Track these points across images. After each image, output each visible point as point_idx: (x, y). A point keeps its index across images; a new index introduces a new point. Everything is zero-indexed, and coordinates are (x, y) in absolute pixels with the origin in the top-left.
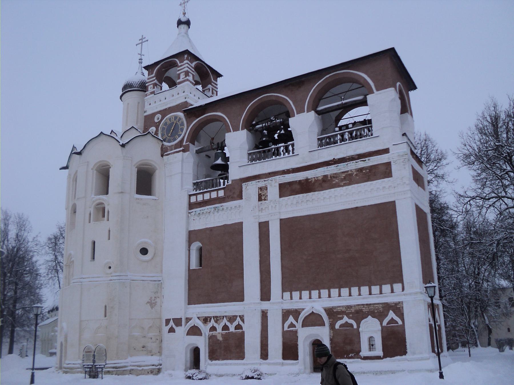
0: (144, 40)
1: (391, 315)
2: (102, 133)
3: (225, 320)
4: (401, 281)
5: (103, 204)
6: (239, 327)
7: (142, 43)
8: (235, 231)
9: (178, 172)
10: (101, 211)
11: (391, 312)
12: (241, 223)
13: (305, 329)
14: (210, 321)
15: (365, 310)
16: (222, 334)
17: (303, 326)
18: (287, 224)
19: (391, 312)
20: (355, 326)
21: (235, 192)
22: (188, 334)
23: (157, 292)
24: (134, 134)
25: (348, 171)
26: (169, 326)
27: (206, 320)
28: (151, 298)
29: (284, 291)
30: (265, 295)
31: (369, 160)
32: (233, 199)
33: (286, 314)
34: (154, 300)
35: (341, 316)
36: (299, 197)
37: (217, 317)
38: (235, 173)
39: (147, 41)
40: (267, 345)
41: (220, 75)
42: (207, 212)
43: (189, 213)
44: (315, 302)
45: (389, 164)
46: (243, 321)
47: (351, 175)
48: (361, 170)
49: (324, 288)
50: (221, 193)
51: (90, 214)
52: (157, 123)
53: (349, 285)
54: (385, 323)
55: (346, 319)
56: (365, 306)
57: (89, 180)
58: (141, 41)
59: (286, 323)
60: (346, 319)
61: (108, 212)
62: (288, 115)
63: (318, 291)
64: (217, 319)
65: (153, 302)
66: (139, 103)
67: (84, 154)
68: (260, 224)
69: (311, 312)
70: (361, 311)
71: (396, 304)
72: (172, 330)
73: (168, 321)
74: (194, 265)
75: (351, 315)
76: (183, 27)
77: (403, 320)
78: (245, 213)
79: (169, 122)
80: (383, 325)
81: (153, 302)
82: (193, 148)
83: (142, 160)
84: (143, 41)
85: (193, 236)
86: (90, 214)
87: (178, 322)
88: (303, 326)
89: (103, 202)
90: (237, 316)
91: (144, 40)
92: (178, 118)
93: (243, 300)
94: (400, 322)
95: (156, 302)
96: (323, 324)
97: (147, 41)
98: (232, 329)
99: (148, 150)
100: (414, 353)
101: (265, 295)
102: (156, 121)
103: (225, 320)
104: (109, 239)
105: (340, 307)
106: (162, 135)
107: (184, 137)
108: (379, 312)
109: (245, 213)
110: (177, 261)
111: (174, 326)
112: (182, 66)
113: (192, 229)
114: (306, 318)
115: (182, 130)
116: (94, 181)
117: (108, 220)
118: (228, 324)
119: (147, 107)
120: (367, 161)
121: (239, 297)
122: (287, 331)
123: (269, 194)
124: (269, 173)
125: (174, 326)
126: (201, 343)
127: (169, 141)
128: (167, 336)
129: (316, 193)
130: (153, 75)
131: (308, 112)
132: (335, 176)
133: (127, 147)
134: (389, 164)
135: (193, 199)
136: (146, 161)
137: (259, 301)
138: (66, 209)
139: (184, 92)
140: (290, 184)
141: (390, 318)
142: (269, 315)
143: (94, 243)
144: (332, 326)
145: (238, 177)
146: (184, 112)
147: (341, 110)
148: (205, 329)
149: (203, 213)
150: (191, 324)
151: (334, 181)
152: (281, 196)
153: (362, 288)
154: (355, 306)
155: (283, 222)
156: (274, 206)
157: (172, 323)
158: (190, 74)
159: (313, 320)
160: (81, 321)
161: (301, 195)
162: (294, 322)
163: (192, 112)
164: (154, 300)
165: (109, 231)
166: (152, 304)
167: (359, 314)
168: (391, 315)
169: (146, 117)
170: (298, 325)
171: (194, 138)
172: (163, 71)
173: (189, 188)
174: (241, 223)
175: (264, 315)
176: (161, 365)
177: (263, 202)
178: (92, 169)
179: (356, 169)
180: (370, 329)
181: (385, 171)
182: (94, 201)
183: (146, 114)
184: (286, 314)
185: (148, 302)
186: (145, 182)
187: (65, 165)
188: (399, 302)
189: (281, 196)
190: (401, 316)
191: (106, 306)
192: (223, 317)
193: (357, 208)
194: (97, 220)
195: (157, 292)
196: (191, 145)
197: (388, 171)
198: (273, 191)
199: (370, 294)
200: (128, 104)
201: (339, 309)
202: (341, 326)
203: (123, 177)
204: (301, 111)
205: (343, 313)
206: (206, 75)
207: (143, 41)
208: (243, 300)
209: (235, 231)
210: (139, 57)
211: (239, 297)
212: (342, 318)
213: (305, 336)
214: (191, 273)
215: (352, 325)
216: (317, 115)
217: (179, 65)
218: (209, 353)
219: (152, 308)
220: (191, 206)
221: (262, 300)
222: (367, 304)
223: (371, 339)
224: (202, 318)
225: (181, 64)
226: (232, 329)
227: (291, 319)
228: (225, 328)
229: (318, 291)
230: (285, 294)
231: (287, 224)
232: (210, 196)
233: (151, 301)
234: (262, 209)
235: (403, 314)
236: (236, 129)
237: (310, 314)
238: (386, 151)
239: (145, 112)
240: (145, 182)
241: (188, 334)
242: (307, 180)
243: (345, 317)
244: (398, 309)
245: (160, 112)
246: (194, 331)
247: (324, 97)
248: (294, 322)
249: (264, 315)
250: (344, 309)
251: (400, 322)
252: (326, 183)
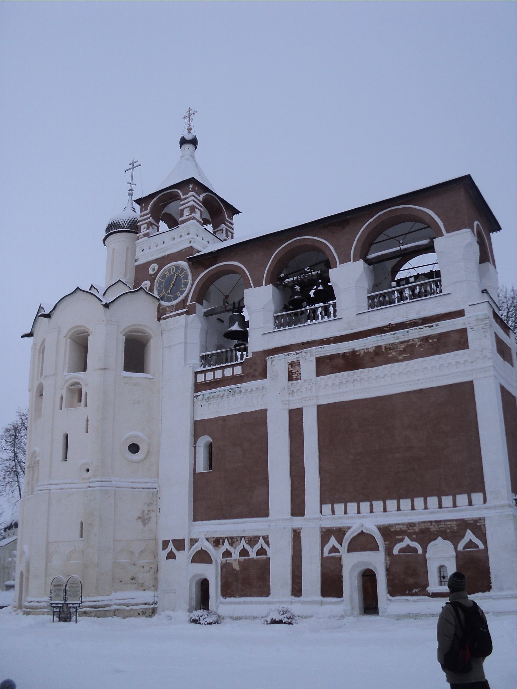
0: (135, 165)
1: (469, 536)
2: (78, 288)
3: (243, 543)
5: (79, 384)
6: (262, 552)
7: (132, 168)
8: (257, 421)
9: (180, 342)
10: (77, 394)
11: (469, 532)
12: (266, 410)
13: (352, 554)
14: (223, 544)
15: (433, 528)
16: (239, 562)
17: (349, 551)
18: (325, 412)
19: (469, 532)
20: (420, 551)
21: (256, 369)
22: (193, 561)
23: (151, 504)
24: (122, 289)
25: (408, 341)
26: (168, 550)
27: (217, 542)
28: (143, 511)
29: (323, 502)
30: (298, 508)
31: (437, 325)
32: (254, 378)
33: (326, 534)
34: (148, 514)
35: (401, 537)
36: (343, 375)
37: (232, 538)
38: (256, 343)
39: (140, 165)
40: (300, 577)
41: (238, 212)
42: (218, 396)
43: (195, 397)
44: (366, 518)
45: (464, 331)
46: (268, 543)
48: (426, 339)
49: (377, 499)
50: (238, 370)
51: (62, 398)
52: (152, 275)
53: (411, 495)
54: (460, 547)
55: (407, 541)
56: (433, 524)
57: (62, 352)
58: (131, 166)
59: (327, 546)
60: (407, 541)
61: (86, 395)
62: (328, 264)
63: (368, 503)
64: (232, 541)
65: (146, 517)
66: (128, 248)
67: (54, 317)
68: (291, 412)
69: (359, 531)
70: (428, 529)
71: (476, 521)
72: (171, 556)
73: (166, 544)
74: (201, 468)
75: (414, 536)
76: (188, 147)
77: (485, 543)
78: (271, 397)
79: (168, 274)
80: (458, 550)
81: (146, 517)
82: (201, 309)
83: (133, 325)
84: (134, 165)
85: (199, 428)
86: (62, 398)
87: (179, 544)
88: (349, 551)
89: (78, 381)
90: (259, 537)
91: (135, 165)
92: (180, 269)
93: (267, 515)
94: (481, 546)
95: (150, 518)
96: (377, 549)
97: (140, 165)
98: (253, 554)
99: (140, 312)
100: (501, 589)
101: (298, 508)
102: (151, 272)
103: (243, 543)
104: (87, 432)
105: (399, 524)
106: (159, 292)
108: (452, 532)
109: (271, 397)
110: (178, 462)
111: (174, 550)
112: (186, 199)
113: (198, 418)
114: (354, 539)
115: (186, 285)
116: (68, 355)
117: (86, 406)
118: (248, 547)
119: (139, 254)
120: (435, 327)
121: (262, 510)
122: (327, 558)
123: (302, 372)
124: (303, 344)
125: (174, 550)
126: (211, 573)
127: (168, 300)
128: (164, 564)
129: (366, 370)
130: (148, 211)
131: (354, 261)
132: (390, 347)
133: (112, 307)
134: (464, 331)
135: (200, 378)
136: (138, 327)
137: (289, 516)
138: (29, 391)
139: (188, 234)
140: (331, 358)
141: (468, 540)
142: (303, 535)
143: (67, 437)
144: (389, 551)
145: (260, 349)
146: (189, 260)
147: (399, 259)
148: (216, 554)
149: (213, 396)
150: (197, 547)
151: (391, 353)
152: (318, 375)
153: (429, 499)
154: (419, 523)
156: (309, 387)
157: (171, 546)
158: (196, 210)
159: (363, 542)
160: (48, 543)
161: (345, 373)
162: (337, 546)
163: (199, 262)
164: (148, 514)
165: (88, 421)
166: (144, 519)
168: (469, 536)
169: (137, 267)
170: (343, 550)
171: (201, 295)
172: (161, 206)
173: (195, 362)
174: (266, 410)
175: (297, 535)
176: (156, 603)
177: (295, 382)
178: (65, 337)
179: (419, 338)
181: (459, 341)
182: (67, 381)
183: (137, 263)
184: (326, 534)
185: (139, 518)
186: (136, 354)
187: (29, 332)
188: (480, 519)
189: (318, 375)
190: (483, 537)
191: (82, 523)
192: (241, 538)
193: (421, 389)
194: (71, 405)
195: (151, 504)
196: (197, 304)
197: (462, 340)
199: (440, 507)
200: (114, 249)
201: (398, 528)
202: (401, 551)
203: (106, 347)
204: (345, 259)
205: (403, 533)
206: (218, 211)
207: (134, 165)
208: (267, 515)
209: (257, 421)
210: (129, 187)
211: (262, 510)
212: (402, 540)
213: (352, 564)
214: (197, 477)
215: (415, 550)
216: (366, 265)
217: (182, 197)
218: (222, 587)
219: (144, 525)
220: (198, 387)
221: (294, 514)
222: (436, 522)
224: (213, 540)
225: (185, 196)
226: (253, 554)
227: (333, 541)
228: (244, 553)
229: (368, 503)
230: (324, 506)
231: (325, 412)
232: (223, 374)
233: (144, 516)
234: (293, 391)
235: (485, 535)
236: (258, 284)
237: (359, 535)
238: (460, 313)
239: (136, 260)
240: (136, 354)
241: (193, 561)
242: (354, 352)
243: (406, 538)
244: (478, 527)
245: (156, 261)
246: (202, 557)
247: (378, 240)
248: (337, 546)
249: (297, 535)
250: (404, 528)
251: (481, 546)
252: (379, 357)
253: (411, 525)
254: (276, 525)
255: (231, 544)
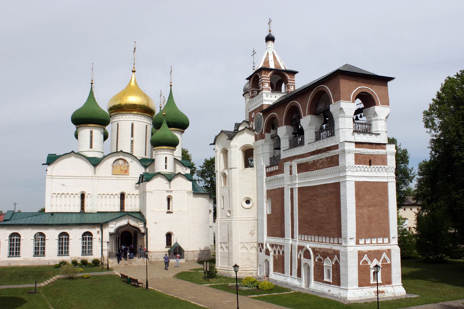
2: (222, 131)
4: (341, 237)
6: (283, 252)
11: (336, 256)
12: (284, 188)
27: (272, 246)
45: (338, 156)
47: (324, 161)
48: (327, 158)
60: (319, 257)
64: (276, 246)
98: (281, 253)
103: (279, 247)
107: (262, 130)
124: (294, 156)
155: (299, 189)
167: (325, 254)
180: (328, 264)
198: (295, 169)
205: (317, 252)
208: (284, 237)
219: (252, 236)
223: (329, 271)
226: (281, 253)
227: (300, 252)
253: (320, 249)
254: (288, 241)
255: (276, 247)
